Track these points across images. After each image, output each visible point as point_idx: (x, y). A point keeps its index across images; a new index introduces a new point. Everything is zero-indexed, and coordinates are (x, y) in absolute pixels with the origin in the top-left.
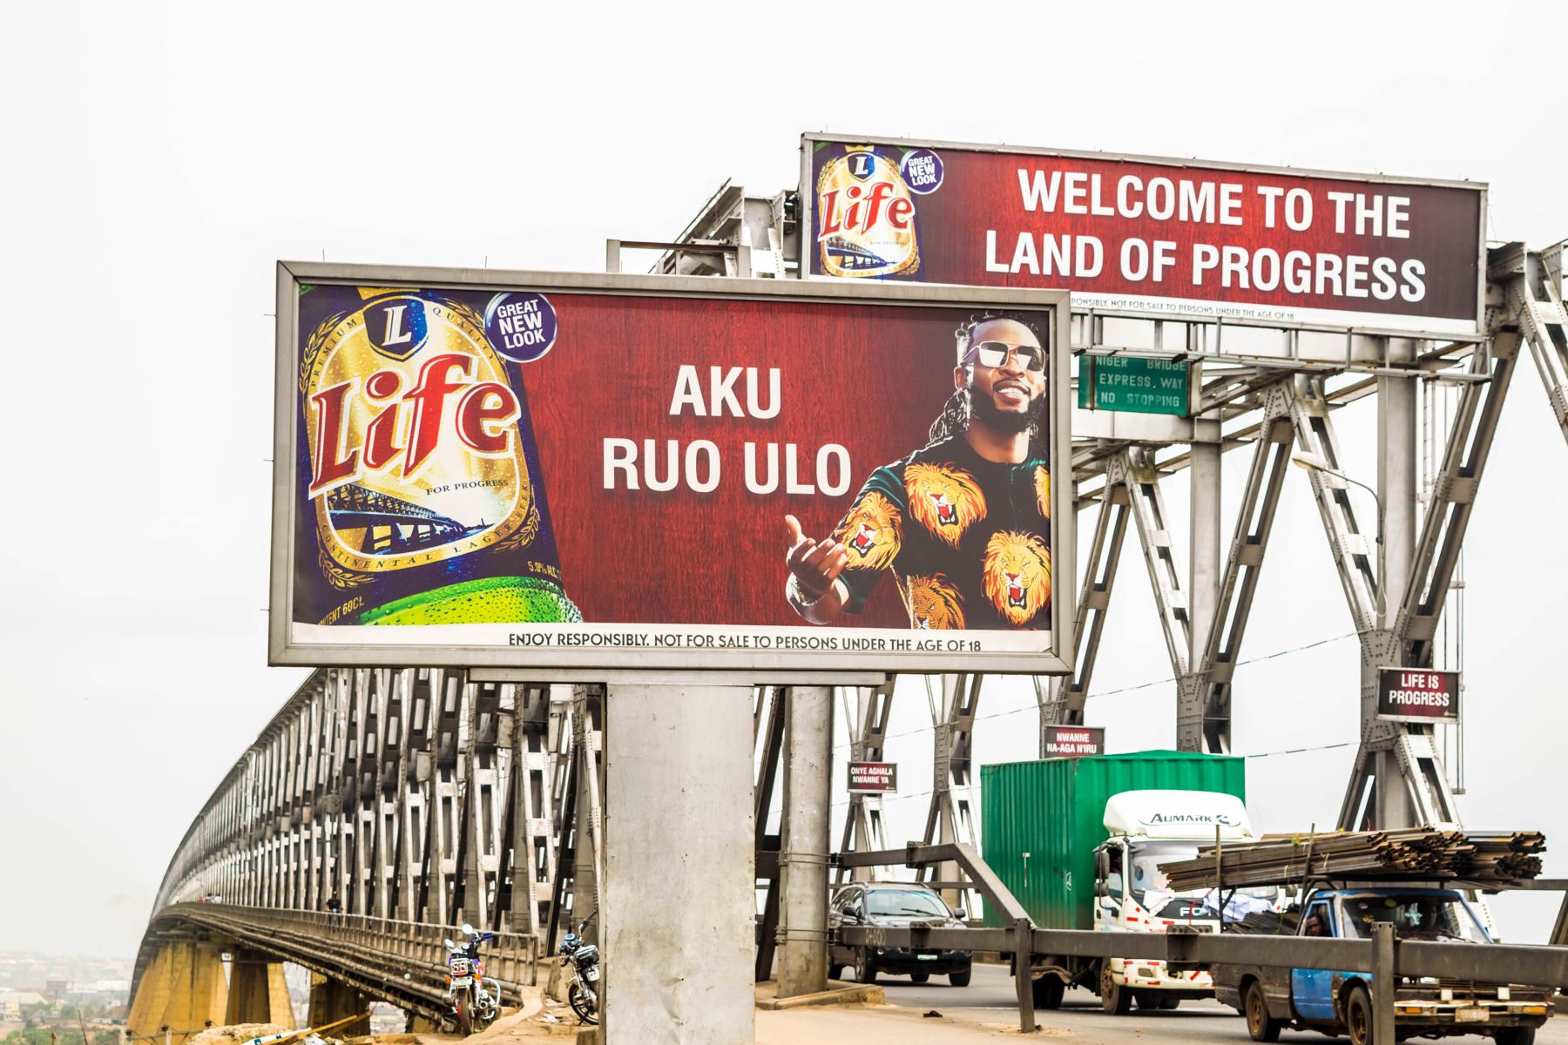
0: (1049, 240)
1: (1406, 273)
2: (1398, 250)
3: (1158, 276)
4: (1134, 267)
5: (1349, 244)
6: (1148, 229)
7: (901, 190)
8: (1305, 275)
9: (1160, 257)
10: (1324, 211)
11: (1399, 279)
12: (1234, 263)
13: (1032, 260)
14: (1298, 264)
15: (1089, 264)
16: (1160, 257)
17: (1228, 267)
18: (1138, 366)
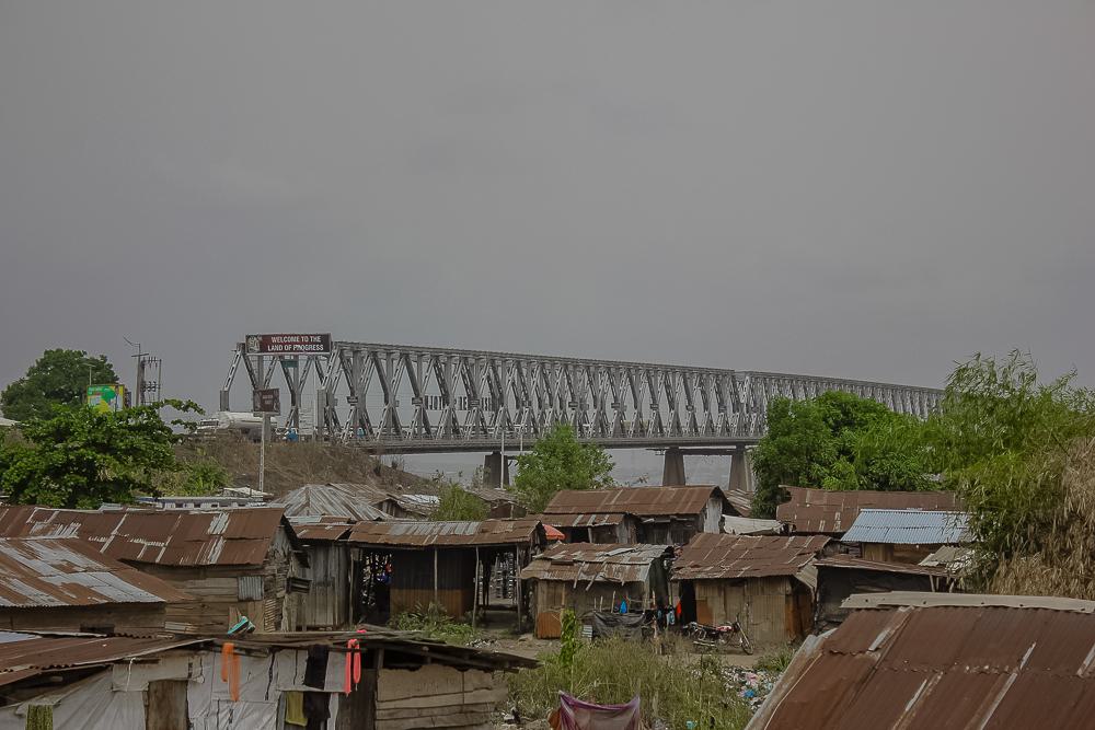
5: (313, 343)
6: (288, 343)
9: (289, 347)
16: (289, 347)
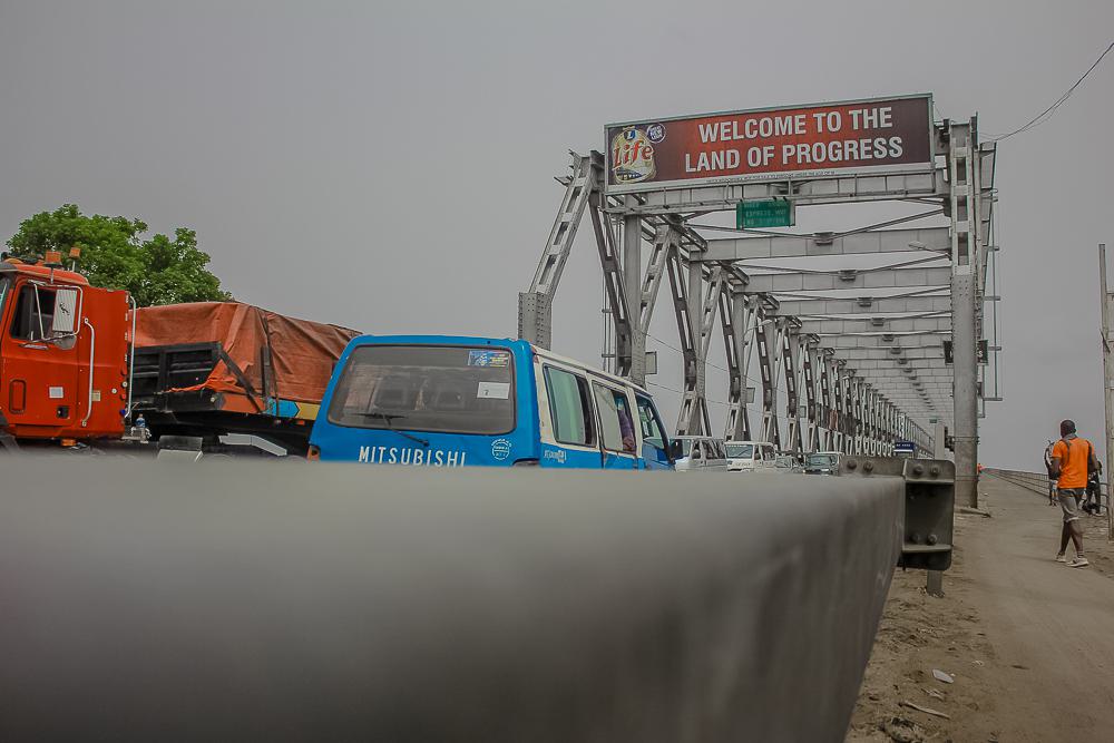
0: (714, 154)
1: (891, 143)
2: (887, 134)
3: (766, 163)
4: (754, 161)
5: (861, 134)
6: (760, 142)
7: (647, 143)
8: (839, 152)
10: (847, 120)
11: (888, 147)
12: (803, 151)
13: (706, 164)
14: (835, 147)
15: (733, 163)
16: (766, 154)
17: (800, 154)
18: (764, 206)
